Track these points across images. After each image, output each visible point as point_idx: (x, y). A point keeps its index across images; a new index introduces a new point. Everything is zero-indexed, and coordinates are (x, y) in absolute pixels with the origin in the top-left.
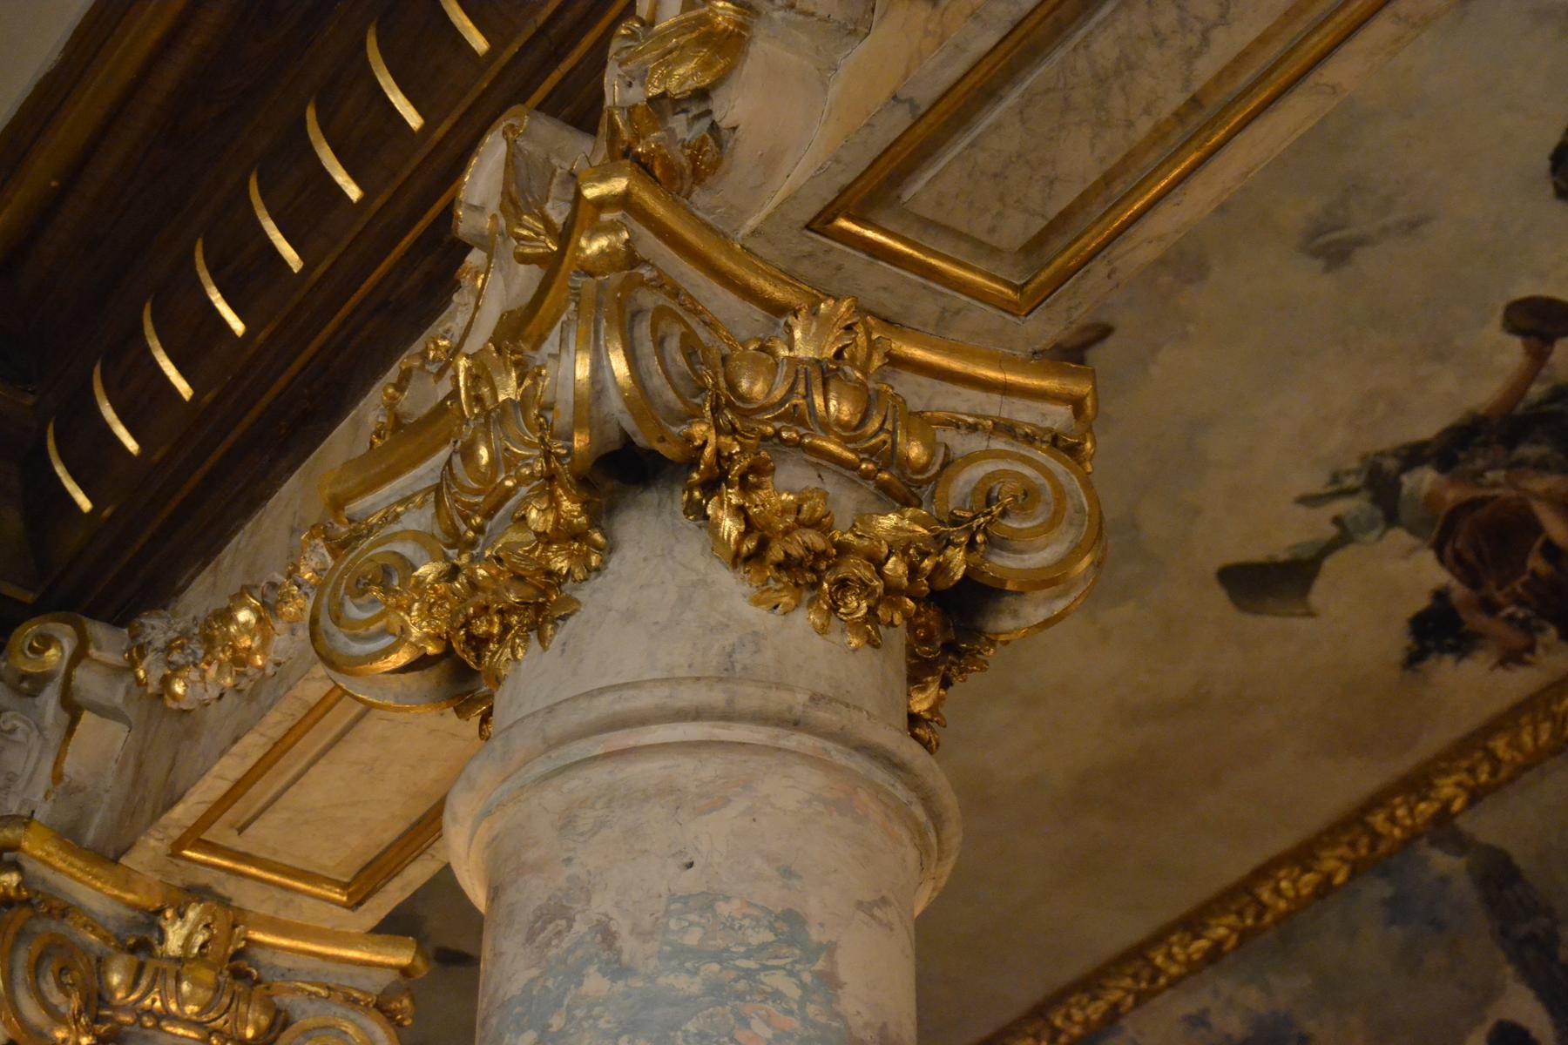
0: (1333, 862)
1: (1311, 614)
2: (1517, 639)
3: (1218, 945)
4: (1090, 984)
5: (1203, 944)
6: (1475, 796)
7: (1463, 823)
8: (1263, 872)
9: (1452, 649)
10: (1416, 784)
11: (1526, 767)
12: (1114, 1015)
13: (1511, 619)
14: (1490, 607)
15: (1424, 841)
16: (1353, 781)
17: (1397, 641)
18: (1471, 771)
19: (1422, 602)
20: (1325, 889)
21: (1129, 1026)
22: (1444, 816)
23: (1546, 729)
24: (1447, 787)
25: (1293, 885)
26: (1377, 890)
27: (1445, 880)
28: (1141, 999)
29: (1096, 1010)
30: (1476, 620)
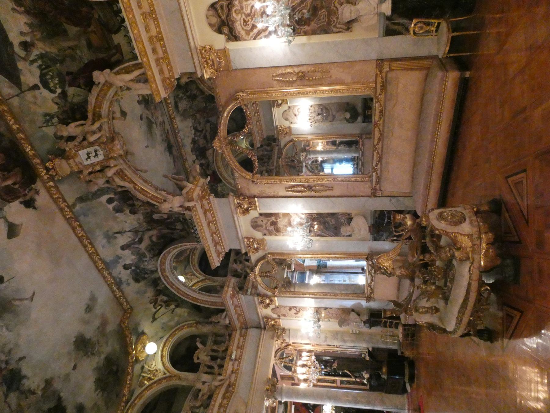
0: (75, 224)
1: (22, 225)
2: (33, 192)
3: (88, 243)
4: (95, 263)
5: (88, 245)
6: (65, 201)
7: (70, 204)
8: (76, 235)
9: (34, 202)
10: (62, 210)
11: (60, 193)
12: (100, 259)
13: (28, 192)
14: (26, 195)
15: (73, 210)
16: (60, 220)
17: (31, 210)
18: (60, 202)
19: (22, 206)
20: (80, 226)
21: (102, 257)
22: (68, 207)
23: (53, 189)
24: (63, 205)
25: (79, 230)
26: (82, 218)
27: (81, 208)
28: (97, 254)
29: (99, 262)
30: (28, 198)
